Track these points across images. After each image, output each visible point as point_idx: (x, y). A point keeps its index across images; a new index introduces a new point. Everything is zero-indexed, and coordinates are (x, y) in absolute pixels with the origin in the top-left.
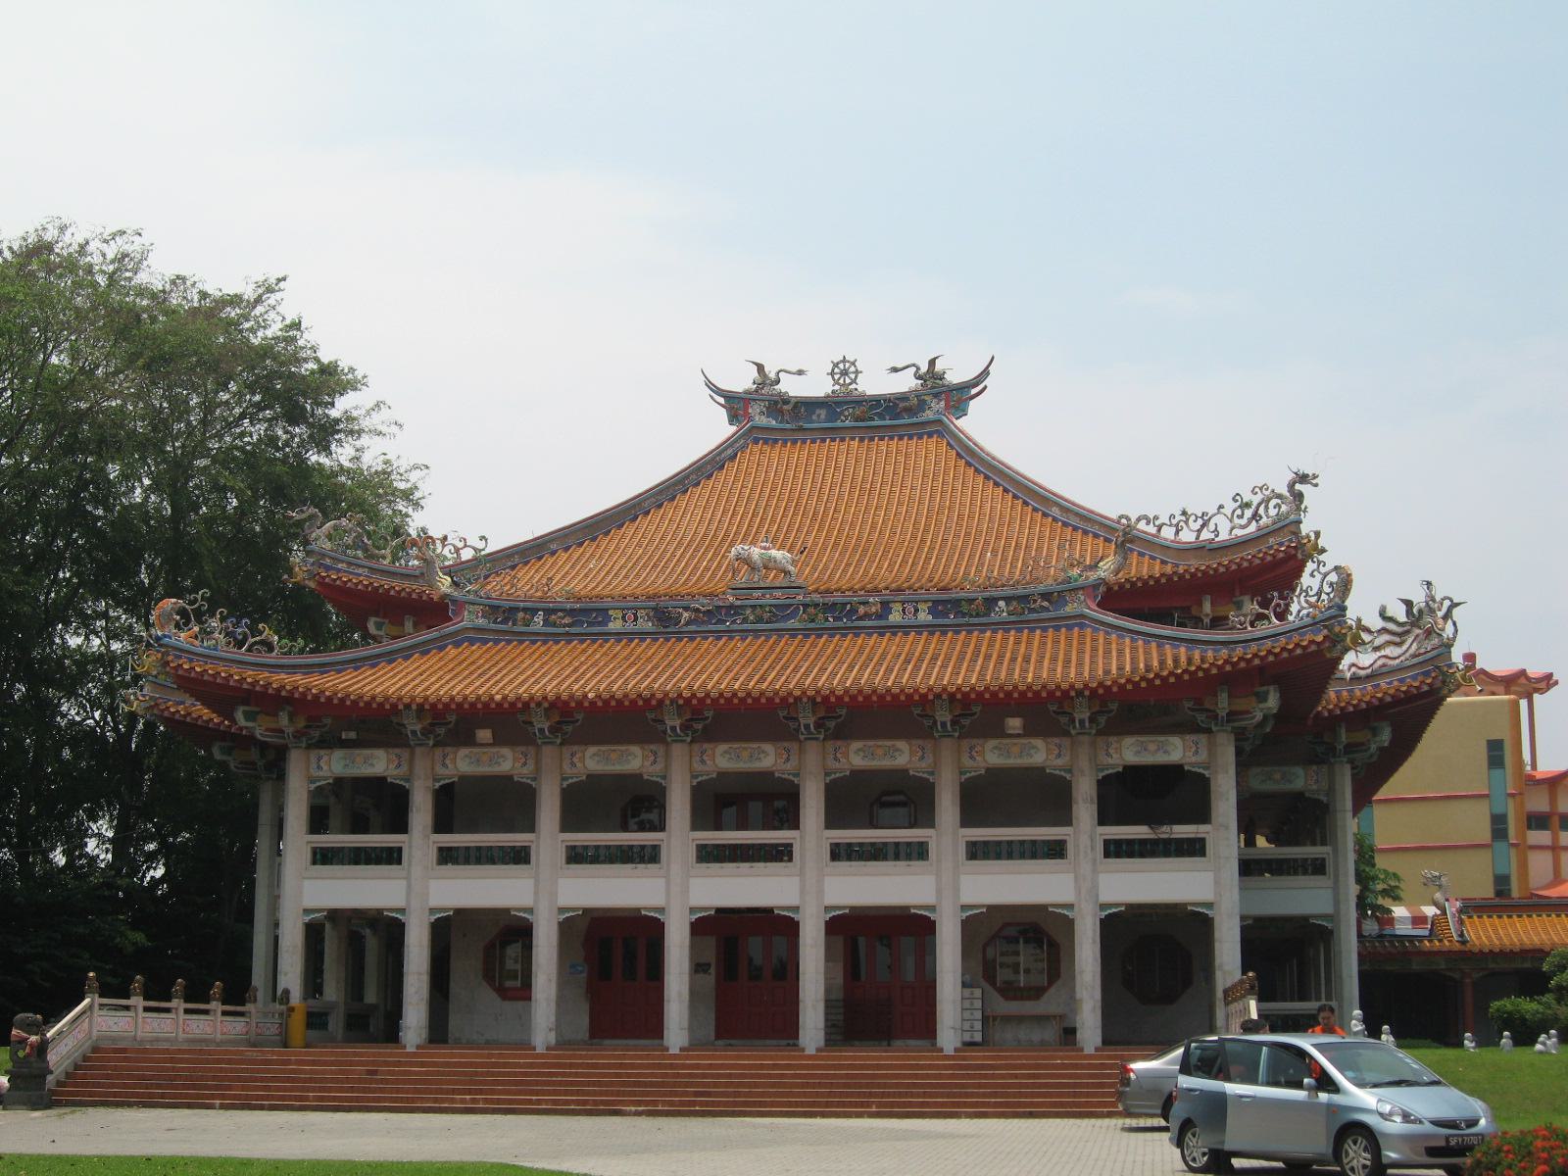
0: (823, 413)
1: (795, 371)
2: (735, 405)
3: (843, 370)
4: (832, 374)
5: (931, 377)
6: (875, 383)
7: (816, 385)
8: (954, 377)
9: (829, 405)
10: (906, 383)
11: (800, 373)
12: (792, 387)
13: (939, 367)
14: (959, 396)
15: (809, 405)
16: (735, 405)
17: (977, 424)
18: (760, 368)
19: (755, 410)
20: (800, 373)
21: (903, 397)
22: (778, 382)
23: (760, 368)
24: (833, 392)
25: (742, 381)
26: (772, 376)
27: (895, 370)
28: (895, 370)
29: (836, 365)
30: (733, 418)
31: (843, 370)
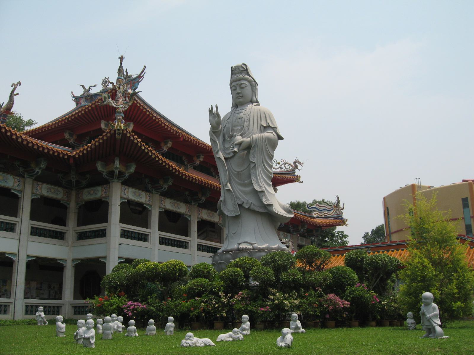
1: (93, 85)
2: (77, 100)
4: (102, 84)
11: (95, 86)
12: (93, 91)
13: (129, 74)
15: (96, 95)
16: (77, 100)
22: (89, 90)
24: (102, 89)
25: (79, 92)
29: (103, 81)
30: (77, 104)
31: (106, 82)
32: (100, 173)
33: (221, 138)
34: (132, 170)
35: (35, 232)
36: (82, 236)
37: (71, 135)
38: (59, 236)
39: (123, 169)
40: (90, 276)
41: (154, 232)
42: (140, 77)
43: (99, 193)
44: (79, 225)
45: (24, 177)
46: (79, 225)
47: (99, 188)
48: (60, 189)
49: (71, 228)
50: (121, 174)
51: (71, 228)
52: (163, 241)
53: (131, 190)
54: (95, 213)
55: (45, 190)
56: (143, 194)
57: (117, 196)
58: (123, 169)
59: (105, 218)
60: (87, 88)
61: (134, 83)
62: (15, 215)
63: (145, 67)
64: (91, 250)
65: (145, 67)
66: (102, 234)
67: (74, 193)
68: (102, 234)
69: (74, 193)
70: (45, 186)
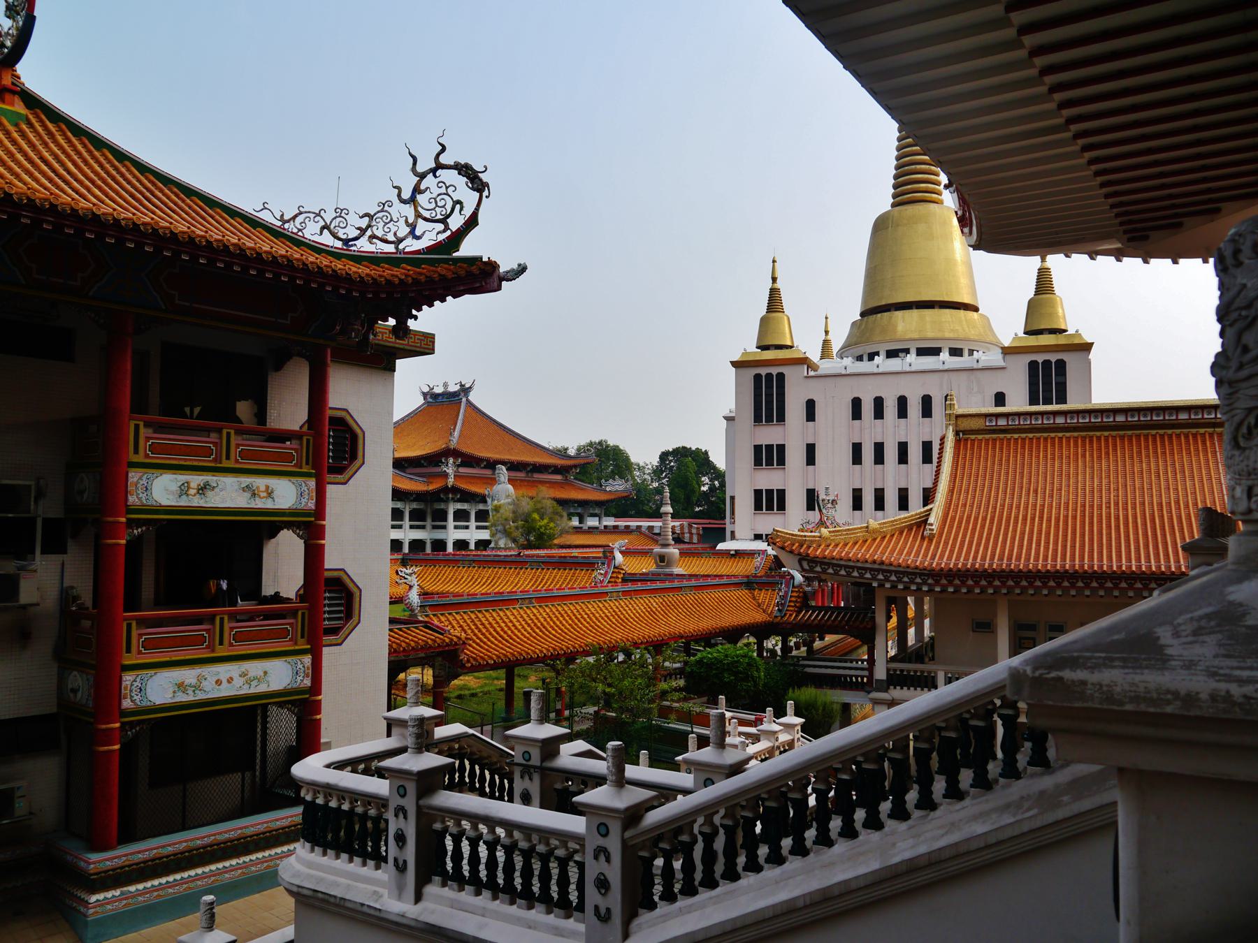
3: (445, 385)
5: (462, 386)
6: (453, 388)
9: (442, 395)
10: (457, 388)
14: (465, 390)
16: (425, 395)
25: (426, 390)
31: (445, 385)
35: (411, 527)
38: (423, 527)
40: (439, 545)
41: (473, 523)
43: (442, 506)
49: (429, 523)
51: (429, 523)
52: (478, 528)
54: (441, 516)
55: (415, 505)
57: (452, 508)
59: (445, 520)
64: (439, 535)
66: (444, 527)
68: (444, 527)
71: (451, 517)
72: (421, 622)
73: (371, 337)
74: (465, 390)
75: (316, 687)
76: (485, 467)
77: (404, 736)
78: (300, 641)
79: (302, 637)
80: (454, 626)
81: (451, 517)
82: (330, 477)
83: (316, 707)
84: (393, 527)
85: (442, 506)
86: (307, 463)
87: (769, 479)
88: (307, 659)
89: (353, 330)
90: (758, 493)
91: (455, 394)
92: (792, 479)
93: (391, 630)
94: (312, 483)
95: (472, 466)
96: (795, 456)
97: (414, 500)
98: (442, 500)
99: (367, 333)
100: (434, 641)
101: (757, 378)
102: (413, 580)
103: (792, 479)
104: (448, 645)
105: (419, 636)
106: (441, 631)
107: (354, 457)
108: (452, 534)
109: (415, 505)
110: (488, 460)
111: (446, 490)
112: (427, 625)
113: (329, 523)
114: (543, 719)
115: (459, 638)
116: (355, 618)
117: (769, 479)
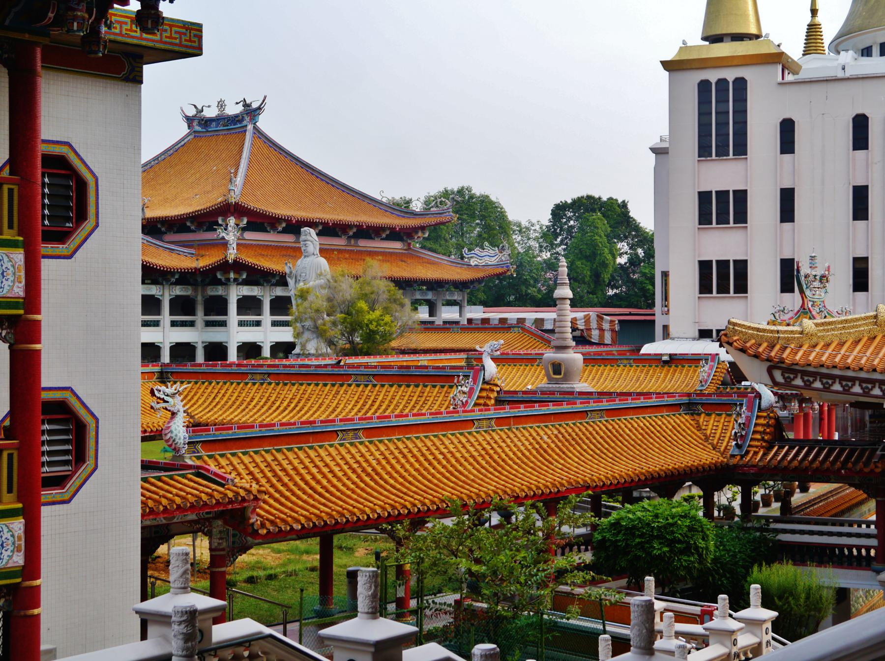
0: (214, 123)
3: (221, 105)
5: (246, 105)
6: (233, 109)
7: (211, 113)
8: (255, 105)
10: (238, 109)
11: (209, 106)
13: (248, 102)
15: (210, 120)
16: (189, 120)
17: (264, 123)
18: (195, 106)
19: (195, 123)
20: (209, 106)
21: (236, 116)
23: (195, 106)
25: (191, 112)
26: (200, 108)
27: (237, 103)
28: (237, 103)
30: (189, 127)
31: (221, 105)
32: (220, 279)
33: (294, 280)
34: (244, 277)
35: (174, 324)
36: (208, 324)
37: (192, 223)
38: (192, 324)
39: (237, 276)
40: (216, 351)
41: (267, 317)
42: (259, 108)
43: (220, 291)
44: (205, 315)
45: (162, 284)
46: (205, 315)
47: (220, 287)
48: (189, 287)
49: (200, 317)
50: (235, 280)
51: (200, 317)
52: (275, 324)
53: (245, 287)
54: (217, 306)
55: (178, 291)
56: (255, 288)
57: (235, 294)
58: (237, 276)
59: (224, 311)
60: (200, 108)
61: (255, 116)
62: (159, 314)
63: (265, 97)
64: (215, 335)
65: (265, 97)
66: (223, 324)
67: (200, 289)
68: (223, 324)
69: (200, 289)
70: (178, 287)
71: (233, 307)
72: (189, 467)
73: (104, 29)
74: (251, 112)
75: (32, 565)
76: (285, 231)
77: (166, 639)
78: (6, 497)
79: (10, 491)
80: (240, 472)
81: (233, 307)
82: (46, 248)
83: (33, 597)
84: (145, 324)
85: (220, 291)
86: (11, 226)
87: (722, 244)
88: (18, 525)
89: (75, 18)
90: (705, 266)
91: (235, 120)
92: (758, 244)
93: (144, 480)
94: (19, 256)
95: (264, 230)
96: (763, 207)
97: (177, 283)
98: (219, 283)
99: (98, 21)
100: (211, 496)
101: (704, 86)
102: (177, 404)
103: (758, 244)
104: (231, 502)
105: (188, 489)
106: (219, 480)
107: (82, 216)
108: (235, 334)
109: (178, 291)
110: (288, 221)
111: (225, 266)
112: (200, 472)
113: (48, 317)
114: (378, 611)
115: (248, 491)
116: (90, 462)
117: (722, 244)
